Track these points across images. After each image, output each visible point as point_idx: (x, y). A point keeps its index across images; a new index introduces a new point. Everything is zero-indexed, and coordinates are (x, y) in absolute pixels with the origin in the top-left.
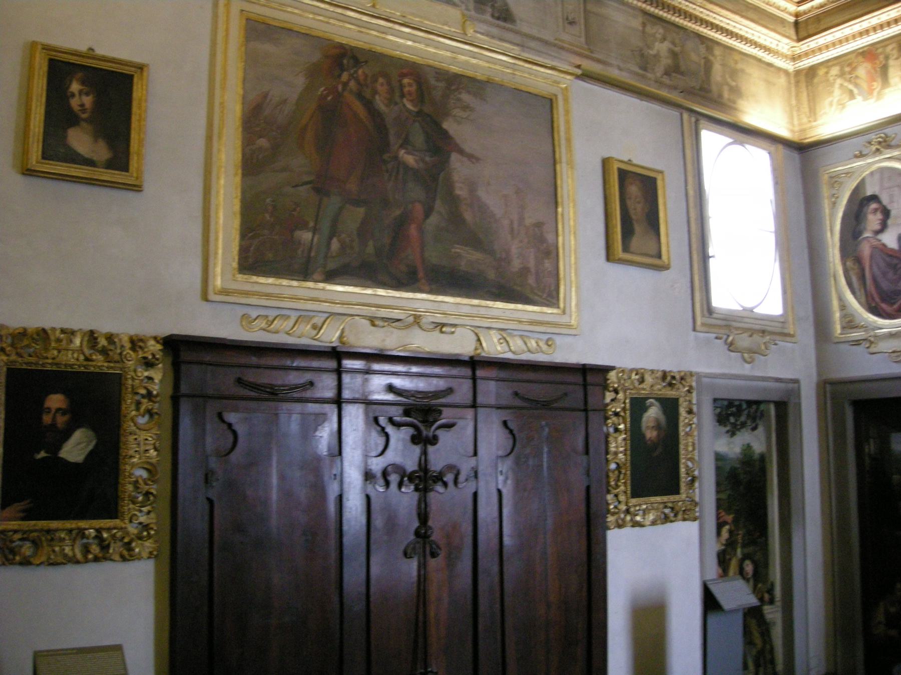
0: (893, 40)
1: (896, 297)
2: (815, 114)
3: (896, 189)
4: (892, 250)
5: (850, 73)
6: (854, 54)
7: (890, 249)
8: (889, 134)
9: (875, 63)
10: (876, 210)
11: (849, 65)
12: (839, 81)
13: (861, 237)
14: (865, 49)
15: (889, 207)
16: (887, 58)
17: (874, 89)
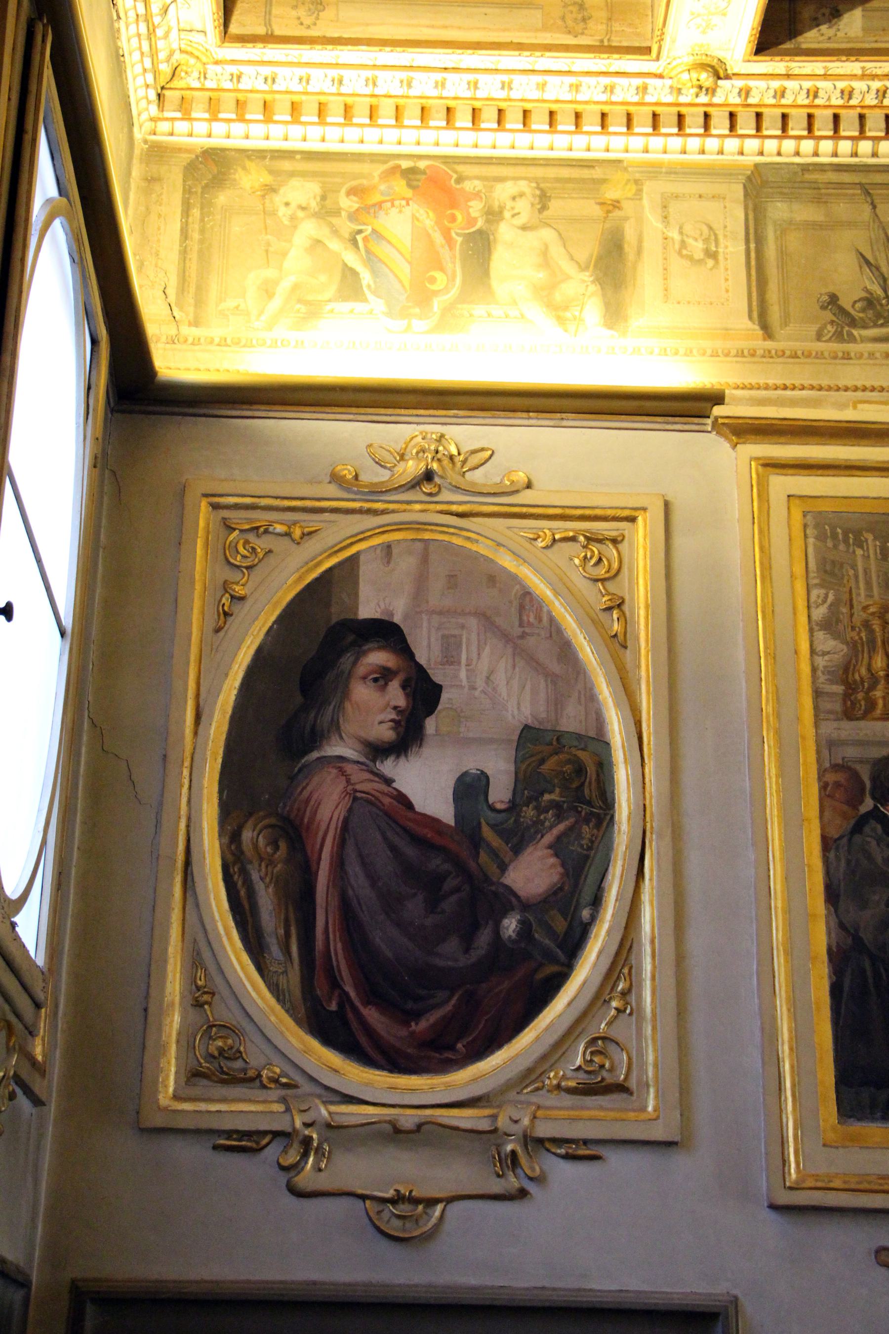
1: (422, 992)
2: (199, 302)
3: (473, 623)
4: (433, 822)
7: (425, 816)
9: (453, 219)
10: (383, 676)
12: (309, 229)
13: (315, 755)
14: (422, 164)
16: (494, 215)
17: (436, 293)
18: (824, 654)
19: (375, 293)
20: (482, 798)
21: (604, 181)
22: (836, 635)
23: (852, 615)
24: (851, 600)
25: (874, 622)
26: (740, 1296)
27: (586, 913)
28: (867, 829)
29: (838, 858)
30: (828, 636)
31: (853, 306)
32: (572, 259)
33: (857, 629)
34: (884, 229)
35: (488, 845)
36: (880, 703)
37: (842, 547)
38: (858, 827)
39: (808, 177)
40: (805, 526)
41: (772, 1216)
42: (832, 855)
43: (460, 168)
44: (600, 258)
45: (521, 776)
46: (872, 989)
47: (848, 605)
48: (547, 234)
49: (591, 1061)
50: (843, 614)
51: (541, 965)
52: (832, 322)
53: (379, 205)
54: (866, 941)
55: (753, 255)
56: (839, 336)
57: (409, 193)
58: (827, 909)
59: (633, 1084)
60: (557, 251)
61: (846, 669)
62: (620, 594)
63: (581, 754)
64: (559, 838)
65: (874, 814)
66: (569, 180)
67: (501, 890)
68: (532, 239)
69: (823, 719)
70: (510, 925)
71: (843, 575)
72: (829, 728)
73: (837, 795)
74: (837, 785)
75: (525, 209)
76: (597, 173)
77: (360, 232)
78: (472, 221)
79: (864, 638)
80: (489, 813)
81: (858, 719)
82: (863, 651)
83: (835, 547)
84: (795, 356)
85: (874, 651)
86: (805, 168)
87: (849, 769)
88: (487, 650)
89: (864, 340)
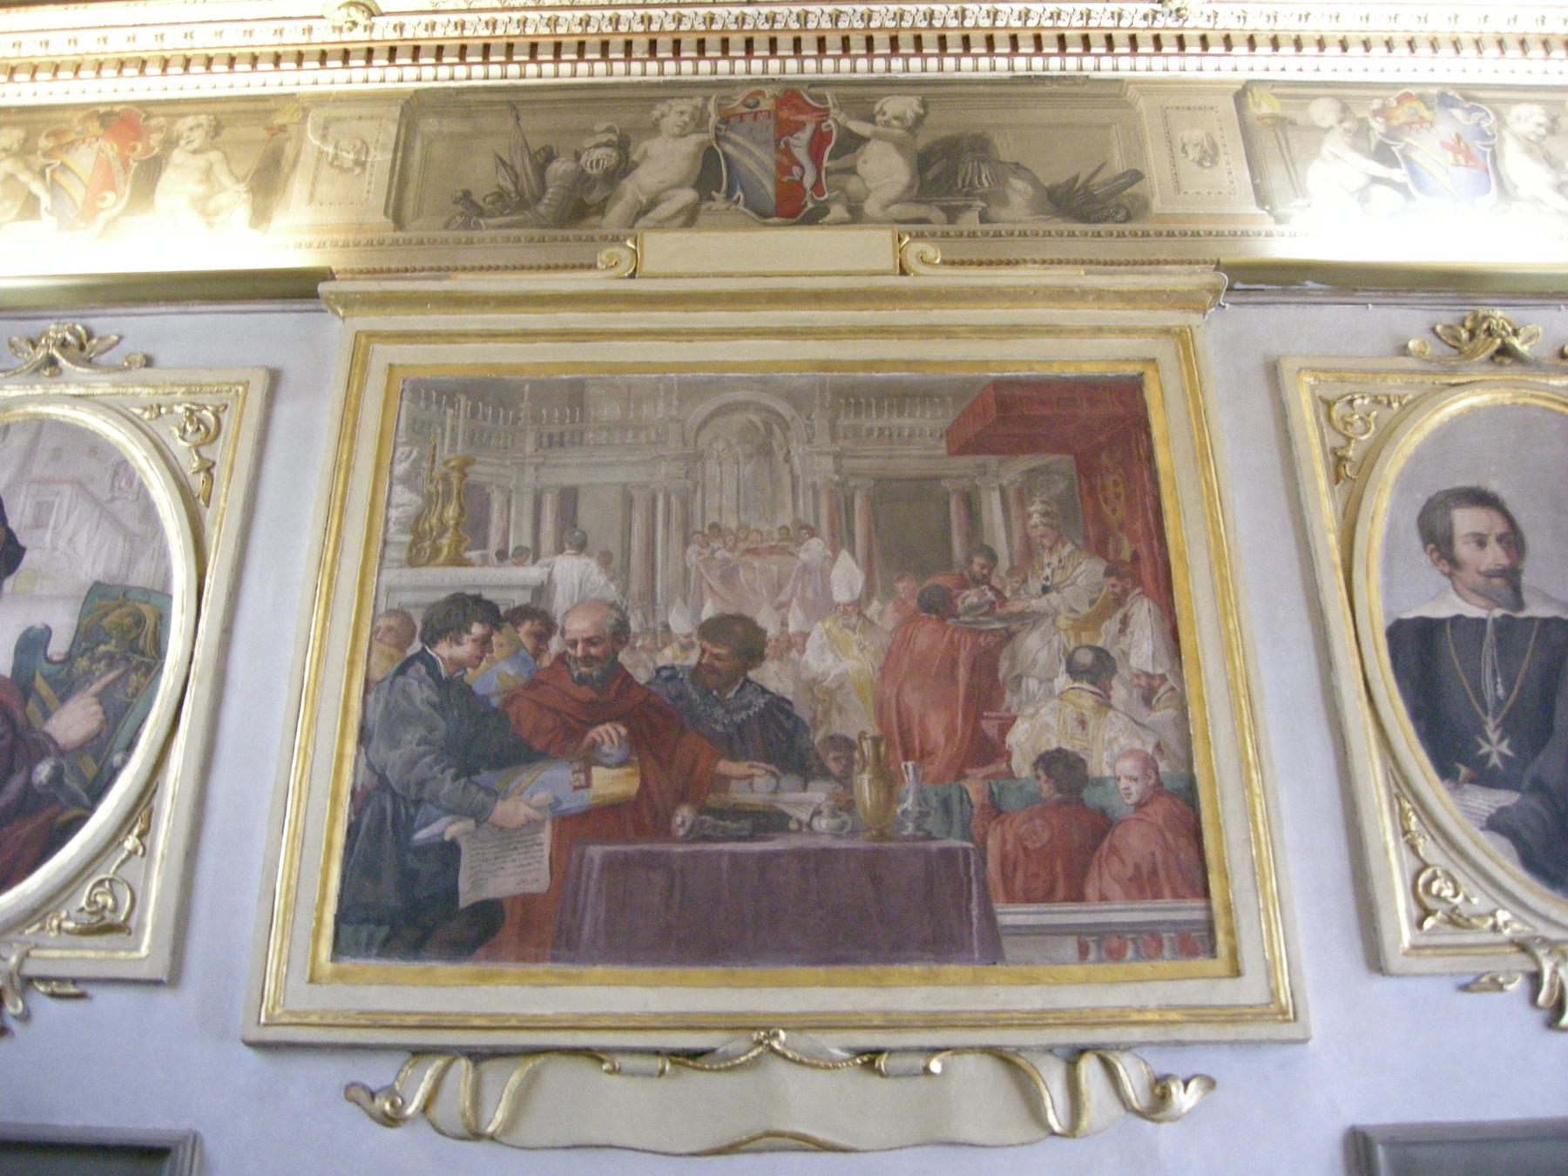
0: (204, 107)
3: (67, 490)
5: (48, 154)
6: (82, 114)
8: (98, 332)
9: (134, 149)
11: (56, 134)
14: (117, 109)
15: (22, 541)
16: (170, 143)
17: (102, 210)
18: (398, 506)
19: (51, 213)
20: (41, 652)
21: (276, 110)
23: (432, 470)
24: (434, 455)
26: (201, 1131)
27: (117, 759)
28: (411, 671)
29: (377, 700)
31: (484, 200)
32: (231, 173)
34: (524, 137)
35: (38, 694)
36: (445, 551)
37: (434, 407)
38: (402, 670)
39: (461, 98)
41: (250, 1053)
43: (150, 109)
44: (258, 172)
45: (82, 629)
46: (389, 828)
48: (215, 156)
49: (95, 902)
51: (63, 809)
52: (462, 214)
53: (72, 143)
55: (398, 162)
56: (466, 226)
57: (100, 131)
59: (133, 923)
60: (221, 172)
61: (418, 519)
62: (212, 458)
63: (145, 609)
64: (106, 687)
65: (422, 656)
66: (245, 112)
67: (41, 737)
68: (200, 161)
70: (43, 771)
74: (390, 629)
75: (198, 138)
76: (271, 105)
77: (49, 165)
78: (149, 149)
80: (46, 666)
81: (422, 565)
83: (427, 407)
84: (421, 243)
86: (460, 91)
88: (76, 513)
89: (488, 227)
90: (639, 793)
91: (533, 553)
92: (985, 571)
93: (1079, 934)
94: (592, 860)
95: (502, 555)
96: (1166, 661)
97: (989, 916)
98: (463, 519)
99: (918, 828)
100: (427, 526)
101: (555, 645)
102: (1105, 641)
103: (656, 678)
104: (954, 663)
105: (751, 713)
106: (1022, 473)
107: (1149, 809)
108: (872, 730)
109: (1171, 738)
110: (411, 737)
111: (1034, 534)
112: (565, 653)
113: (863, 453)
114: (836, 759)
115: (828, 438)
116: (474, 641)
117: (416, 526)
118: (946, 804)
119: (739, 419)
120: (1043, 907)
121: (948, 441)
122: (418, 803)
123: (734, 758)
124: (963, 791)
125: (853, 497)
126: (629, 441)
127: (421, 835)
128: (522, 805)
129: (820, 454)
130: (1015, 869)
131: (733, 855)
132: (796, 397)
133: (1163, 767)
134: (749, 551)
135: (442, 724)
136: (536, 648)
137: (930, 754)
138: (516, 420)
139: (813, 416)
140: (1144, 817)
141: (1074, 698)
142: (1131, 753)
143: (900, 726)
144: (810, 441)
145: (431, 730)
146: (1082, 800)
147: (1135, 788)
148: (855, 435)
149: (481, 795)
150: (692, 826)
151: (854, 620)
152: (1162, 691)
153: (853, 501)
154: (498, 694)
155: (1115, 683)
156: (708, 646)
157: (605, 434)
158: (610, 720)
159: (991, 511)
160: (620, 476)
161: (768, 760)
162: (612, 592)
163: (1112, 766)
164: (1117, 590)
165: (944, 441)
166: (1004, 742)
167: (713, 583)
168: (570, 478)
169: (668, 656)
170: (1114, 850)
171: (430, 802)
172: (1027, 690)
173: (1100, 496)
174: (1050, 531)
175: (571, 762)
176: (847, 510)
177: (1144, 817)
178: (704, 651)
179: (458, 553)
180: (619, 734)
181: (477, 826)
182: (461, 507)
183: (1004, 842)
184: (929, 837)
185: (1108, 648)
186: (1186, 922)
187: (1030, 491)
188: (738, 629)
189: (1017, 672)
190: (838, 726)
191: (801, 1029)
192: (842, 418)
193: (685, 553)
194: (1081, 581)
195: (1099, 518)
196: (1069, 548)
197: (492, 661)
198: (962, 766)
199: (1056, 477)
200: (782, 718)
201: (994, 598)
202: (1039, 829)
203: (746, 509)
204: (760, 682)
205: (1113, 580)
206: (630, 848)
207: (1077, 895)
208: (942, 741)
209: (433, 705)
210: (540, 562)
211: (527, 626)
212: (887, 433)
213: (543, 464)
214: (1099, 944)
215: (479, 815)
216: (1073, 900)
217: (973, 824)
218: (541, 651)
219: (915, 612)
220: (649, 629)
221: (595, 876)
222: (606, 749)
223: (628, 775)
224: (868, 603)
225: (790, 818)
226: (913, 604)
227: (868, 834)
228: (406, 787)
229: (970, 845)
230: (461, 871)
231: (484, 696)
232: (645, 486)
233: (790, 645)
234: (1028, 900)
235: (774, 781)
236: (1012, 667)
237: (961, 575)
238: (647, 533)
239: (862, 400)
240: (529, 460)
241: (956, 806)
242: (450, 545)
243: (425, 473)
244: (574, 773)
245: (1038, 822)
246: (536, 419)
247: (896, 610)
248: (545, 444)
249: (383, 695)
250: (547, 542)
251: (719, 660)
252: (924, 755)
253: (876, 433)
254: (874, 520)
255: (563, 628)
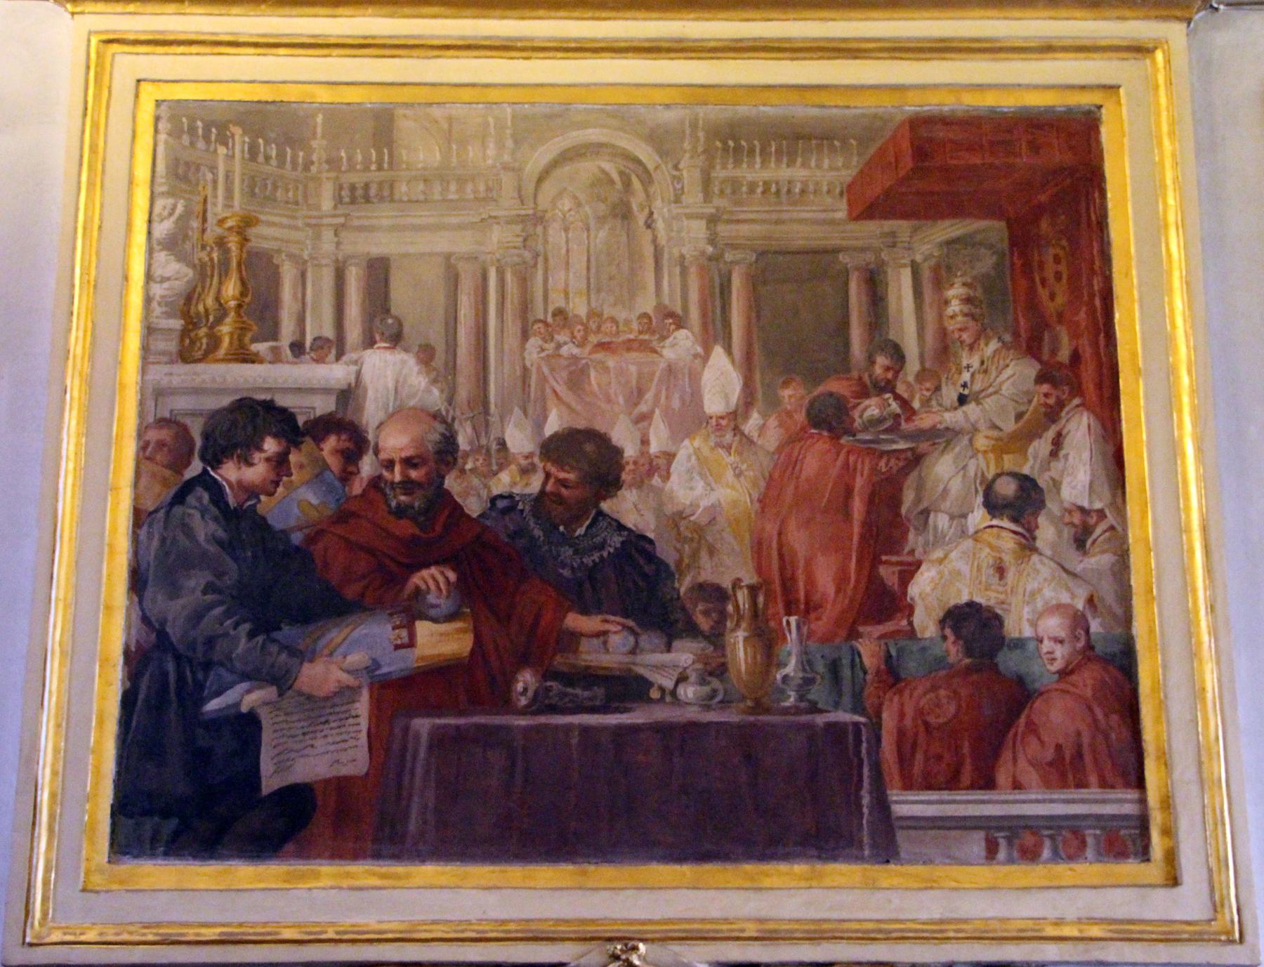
22: (182, 257)
23: (204, 231)
24: (205, 211)
25: (231, 238)
28: (191, 499)
29: (150, 536)
30: (172, 257)
33: (208, 248)
37: (201, 144)
38: (180, 497)
40: (157, 119)
42: (143, 533)
47: (200, 220)
50: (192, 229)
54: (174, 639)
58: (130, 598)
61: (189, 298)
65: (204, 480)
69: (153, 363)
71: (198, 180)
72: (163, 374)
73: (158, 457)
74: (161, 444)
79: (216, 259)
82: (212, 276)
83: (192, 144)
85: (226, 276)
87: (177, 423)
90: (473, 652)
91: (335, 346)
92: (890, 375)
93: (987, 828)
94: (417, 737)
95: (298, 348)
96: (1106, 493)
97: (882, 805)
98: (247, 300)
99: (801, 698)
100: (201, 308)
101: (367, 466)
102: (1032, 468)
103: (490, 509)
104: (849, 492)
105: (605, 554)
106: (941, 245)
107: (1074, 678)
108: (749, 578)
109: (1107, 591)
110: (195, 582)
111: (951, 326)
112: (380, 477)
113: (742, 216)
114: (706, 613)
115: (701, 195)
116: (268, 460)
117: (186, 306)
118: (834, 667)
119: (587, 168)
120: (946, 795)
121: (849, 200)
122: (207, 666)
123: (585, 611)
124: (855, 653)
125: (730, 273)
126: (452, 196)
127: (213, 705)
128: (334, 668)
129: (690, 217)
130: (914, 746)
131: (585, 730)
132: (659, 139)
133: (1095, 626)
134: (602, 346)
135: (232, 566)
136: (344, 470)
137: (818, 607)
138: (308, 165)
139: (681, 166)
140: (1072, 689)
141: (991, 540)
142: (1059, 607)
143: (782, 568)
144: (677, 200)
145: (220, 575)
146: (996, 665)
147: (1060, 652)
148: (734, 192)
149: (284, 656)
150: (536, 693)
151: (729, 437)
152: (1098, 531)
153: (729, 280)
154: (300, 529)
155: (1042, 520)
156: (553, 470)
157: (421, 186)
158: (437, 563)
159: (899, 298)
160: (442, 243)
161: (626, 615)
162: (435, 398)
163: (1034, 624)
164: (1051, 401)
165: (845, 200)
166: (905, 593)
167: (558, 389)
168: (381, 245)
169: (504, 482)
170: (1032, 728)
171: (222, 664)
172: (936, 528)
173: (1037, 279)
174: (971, 324)
175: (391, 615)
176: (722, 293)
177: (1072, 689)
178: (548, 476)
179: (242, 346)
180: (447, 579)
181: (280, 695)
182: (243, 283)
183: (902, 715)
184: (814, 709)
185: (1035, 476)
186: (1114, 817)
187: (949, 268)
188: (589, 448)
189: (924, 505)
190: (708, 572)
191: (665, 939)
192: (718, 167)
193: (523, 348)
194: (1007, 389)
195: (1032, 305)
196: (994, 345)
197: (291, 487)
198: (854, 622)
199: (983, 250)
200: (642, 562)
201: (898, 410)
202: (944, 701)
203: (599, 291)
204: (615, 516)
205: (1045, 388)
206: (462, 721)
207: (988, 783)
208: (831, 590)
209: (220, 543)
210: (345, 358)
211: (331, 443)
212: (773, 189)
213: (343, 225)
214: (1010, 841)
215: (281, 681)
216: (981, 788)
217: (866, 693)
218: (352, 473)
219: (803, 429)
220: (480, 447)
221: (422, 754)
222: (432, 599)
223: (459, 631)
224: (746, 416)
225: (649, 684)
226: (801, 417)
227: (742, 705)
228: (192, 646)
229: (862, 719)
230: (263, 749)
231: (283, 531)
232: (472, 258)
233: (652, 470)
234: (929, 787)
235: (632, 639)
236: (918, 500)
237: (860, 378)
238: (477, 321)
239: (743, 143)
240: (325, 221)
241: (846, 673)
242: (231, 334)
243: (195, 235)
244: (394, 629)
245: (942, 692)
246: (333, 163)
247: (780, 425)
248: (347, 200)
249: (158, 528)
250: (354, 332)
251: (566, 487)
252: (810, 609)
253: (759, 190)
254: (755, 305)
255: (376, 446)
